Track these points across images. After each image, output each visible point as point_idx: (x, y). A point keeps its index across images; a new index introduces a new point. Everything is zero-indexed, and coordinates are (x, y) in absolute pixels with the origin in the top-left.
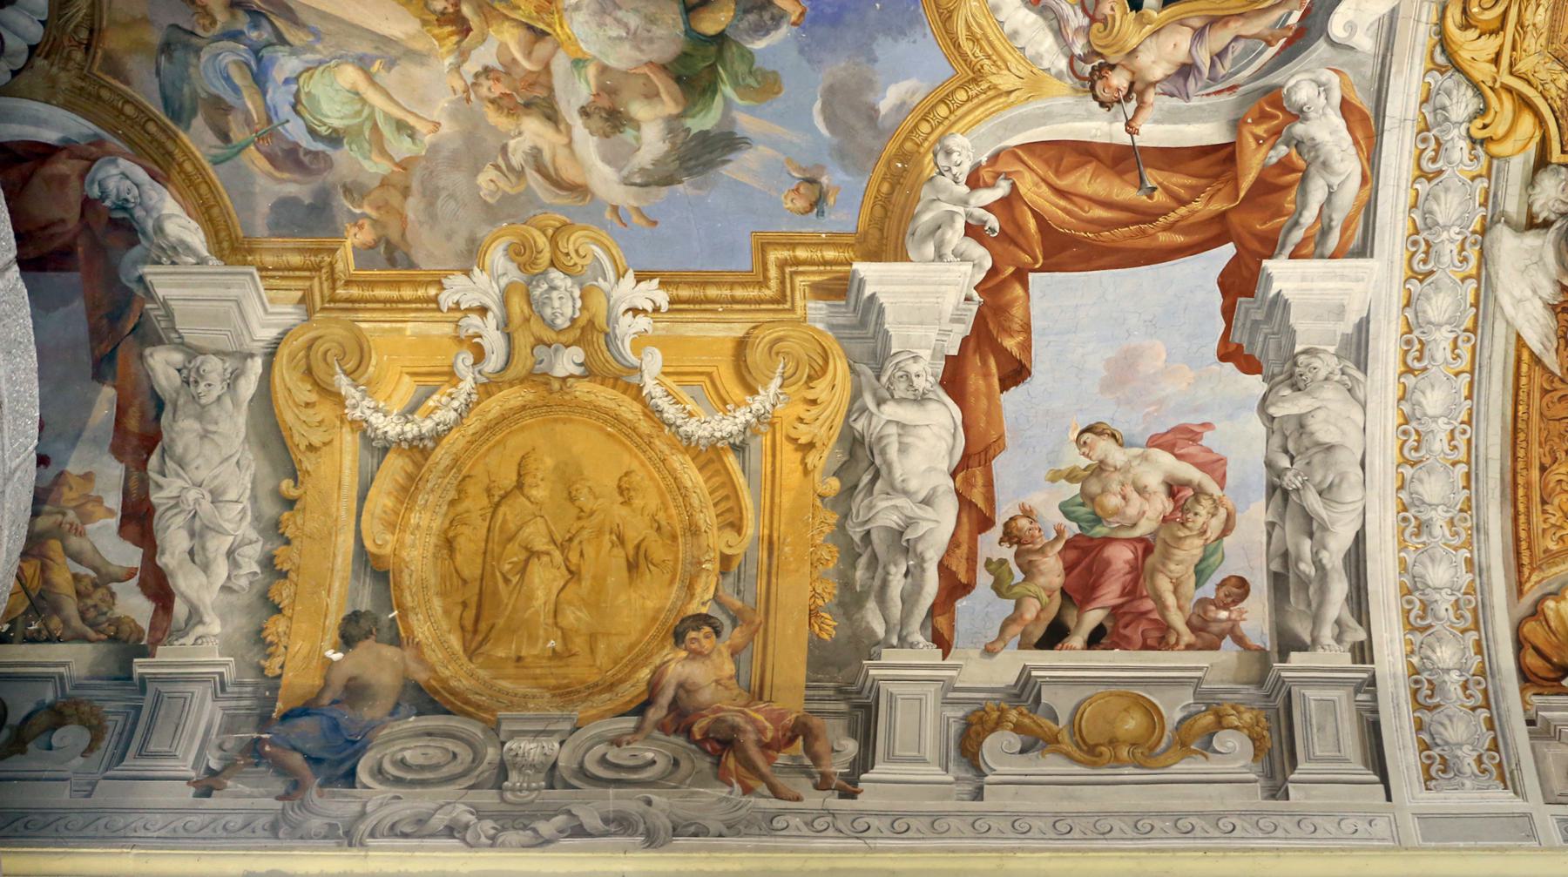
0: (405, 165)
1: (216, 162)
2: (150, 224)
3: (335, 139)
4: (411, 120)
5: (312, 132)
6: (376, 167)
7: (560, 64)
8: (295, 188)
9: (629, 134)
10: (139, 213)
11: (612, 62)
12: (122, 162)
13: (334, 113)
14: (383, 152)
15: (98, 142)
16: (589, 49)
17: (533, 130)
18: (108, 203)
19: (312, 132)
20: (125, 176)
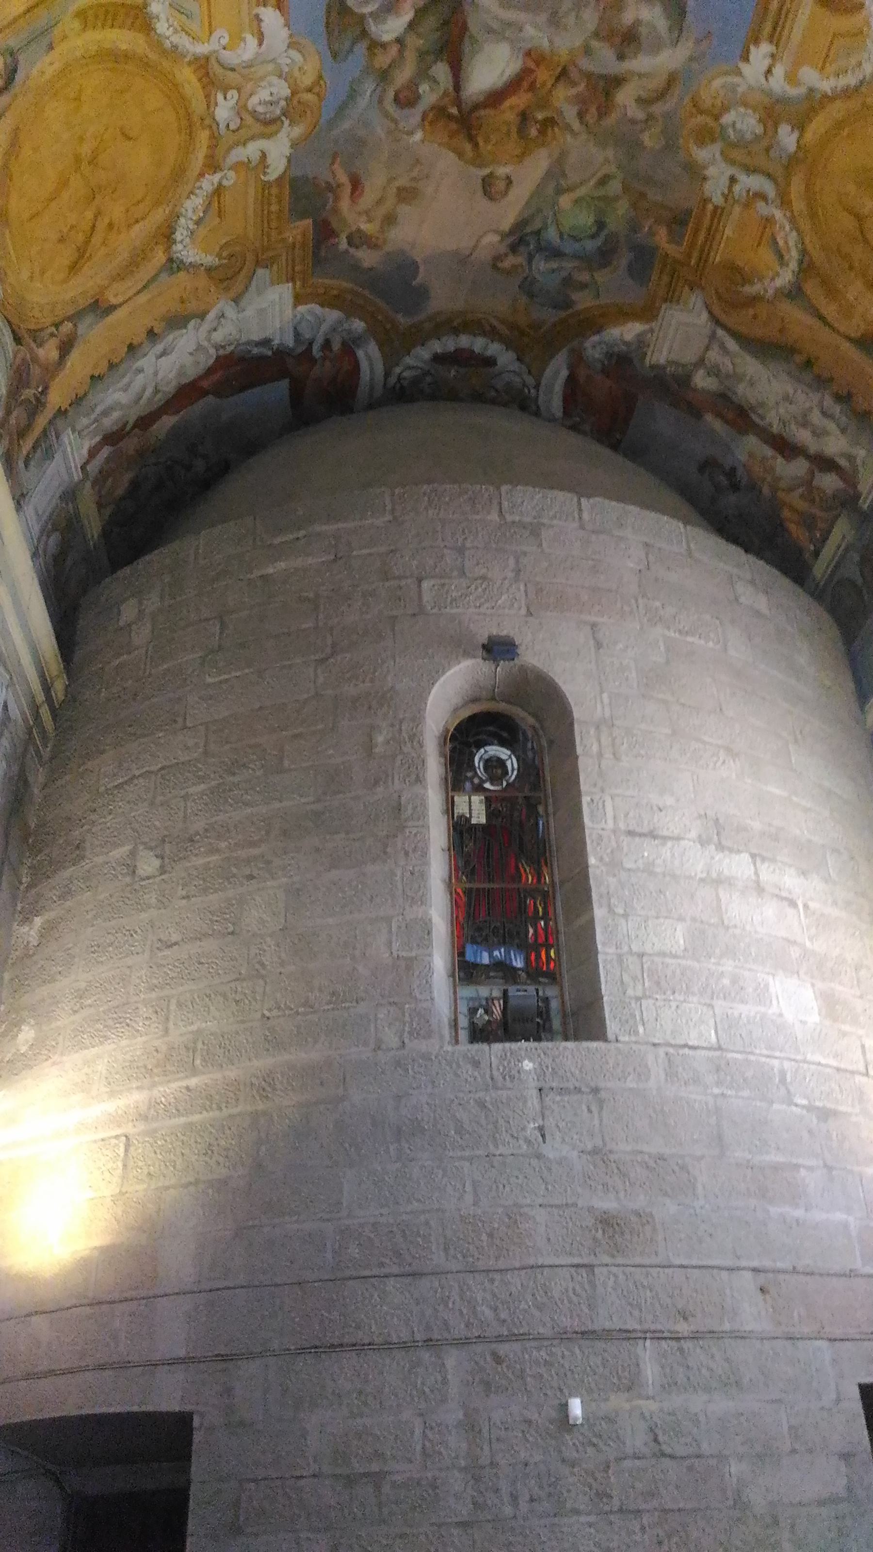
0: (626, 189)
1: (598, 296)
2: (624, 348)
3: (600, 225)
4: (599, 175)
5: (593, 237)
6: (622, 207)
7: (585, 64)
8: (624, 259)
9: (643, 30)
10: (616, 349)
11: (591, 26)
12: (588, 344)
13: (585, 219)
14: (616, 198)
15: (572, 351)
16: (578, 43)
17: (625, 97)
18: (606, 362)
19: (593, 237)
20: (594, 347)
